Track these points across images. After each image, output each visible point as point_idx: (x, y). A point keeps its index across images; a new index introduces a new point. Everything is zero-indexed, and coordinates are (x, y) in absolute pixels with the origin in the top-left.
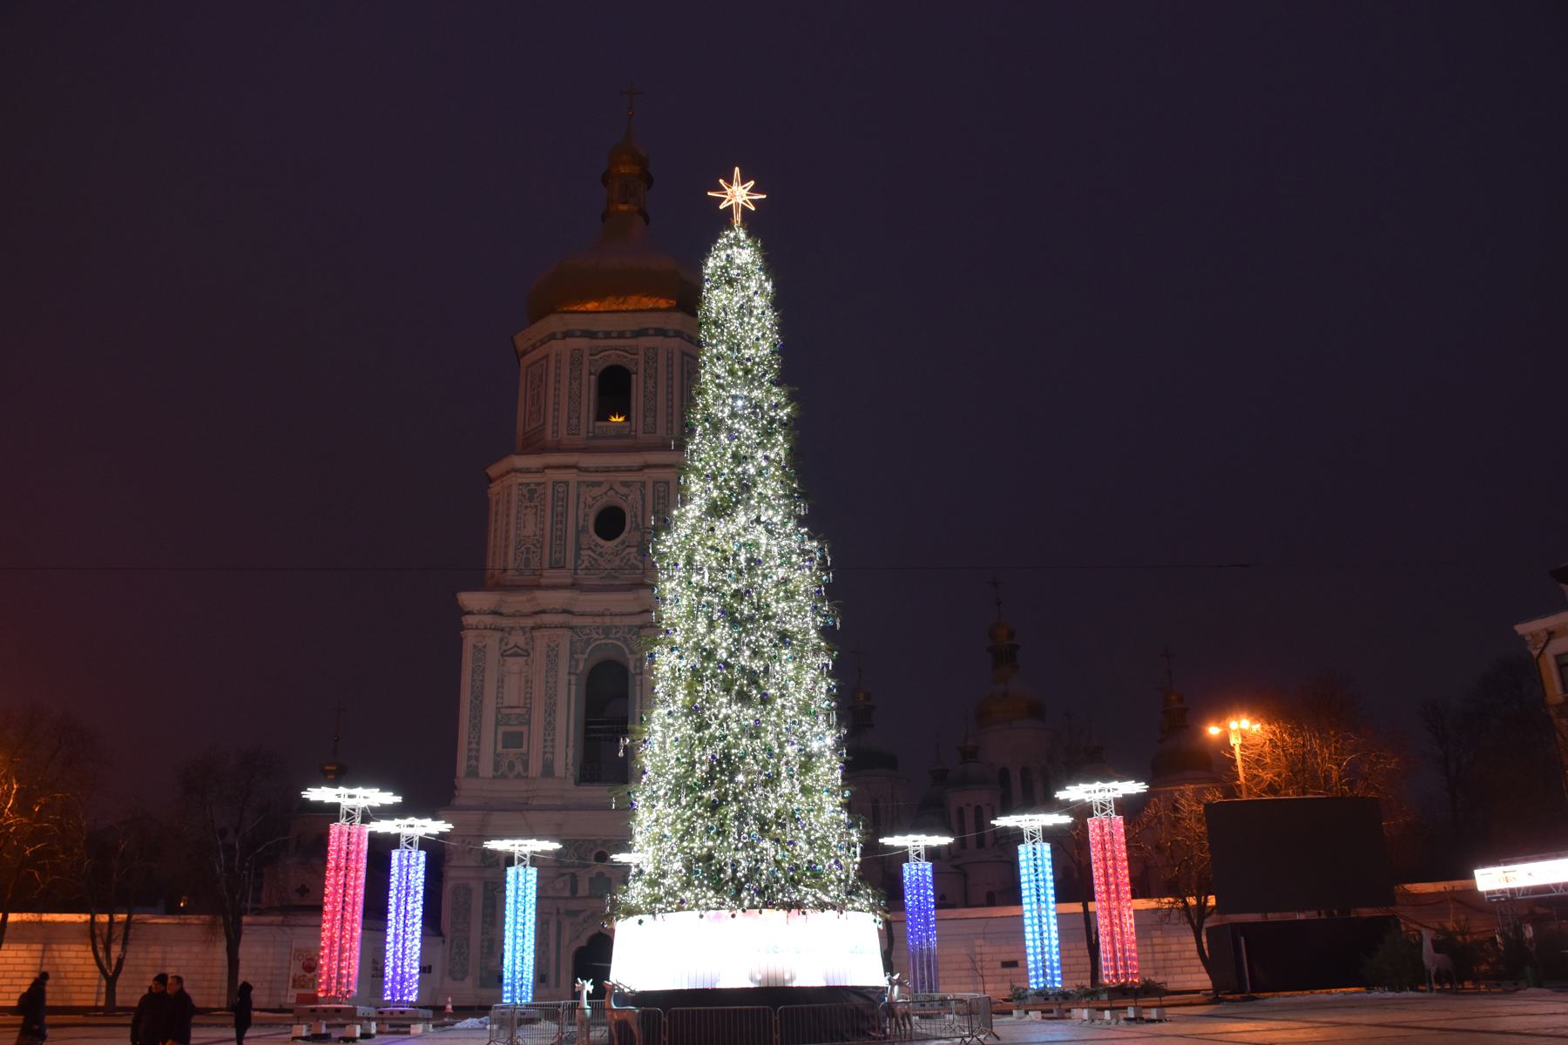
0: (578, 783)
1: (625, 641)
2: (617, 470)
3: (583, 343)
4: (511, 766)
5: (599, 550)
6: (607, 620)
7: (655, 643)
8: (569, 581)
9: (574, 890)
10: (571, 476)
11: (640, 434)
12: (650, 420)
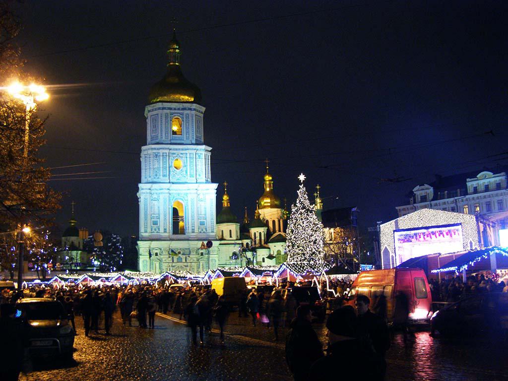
0: (173, 234)
1: (184, 197)
3: (168, 111)
4: (155, 230)
5: (175, 172)
7: (229, 200)
9: (173, 261)
10: (167, 151)
11: (185, 139)
12: (188, 135)
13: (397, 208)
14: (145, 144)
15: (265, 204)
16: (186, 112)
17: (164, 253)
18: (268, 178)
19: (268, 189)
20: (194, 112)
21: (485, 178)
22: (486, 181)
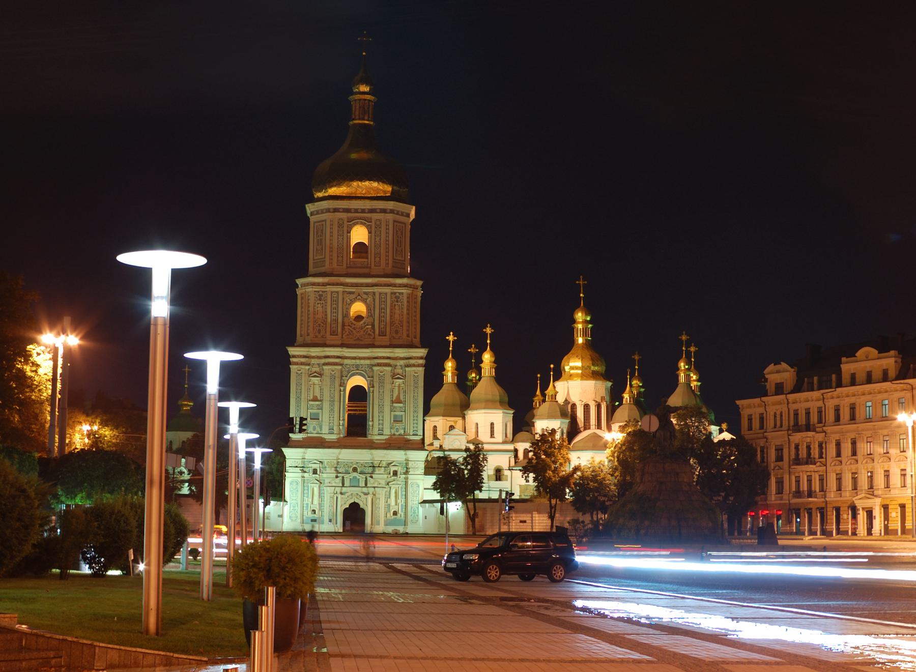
2: (361, 285)
3: (344, 215)
6: (358, 362)
8: (340, 343)
9: (343, 484)
10: (340, 289)
11: (373, 266)
13: (738, 402)
14: (305, 274)
15: (572, 372)
16: (375, 216)
17: (328, 470)
18: (580, 316)
19: (580, 340)
20: (390, 216)
21: (867, 358)
22: (867, 365)
